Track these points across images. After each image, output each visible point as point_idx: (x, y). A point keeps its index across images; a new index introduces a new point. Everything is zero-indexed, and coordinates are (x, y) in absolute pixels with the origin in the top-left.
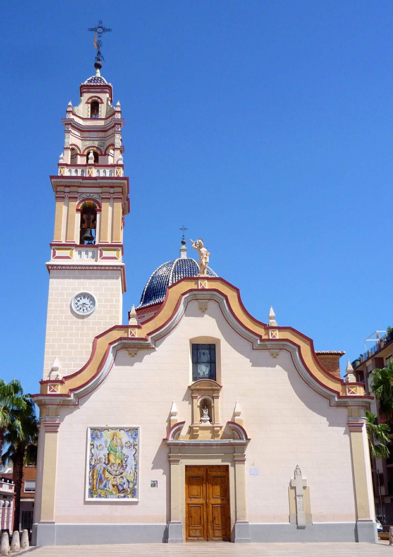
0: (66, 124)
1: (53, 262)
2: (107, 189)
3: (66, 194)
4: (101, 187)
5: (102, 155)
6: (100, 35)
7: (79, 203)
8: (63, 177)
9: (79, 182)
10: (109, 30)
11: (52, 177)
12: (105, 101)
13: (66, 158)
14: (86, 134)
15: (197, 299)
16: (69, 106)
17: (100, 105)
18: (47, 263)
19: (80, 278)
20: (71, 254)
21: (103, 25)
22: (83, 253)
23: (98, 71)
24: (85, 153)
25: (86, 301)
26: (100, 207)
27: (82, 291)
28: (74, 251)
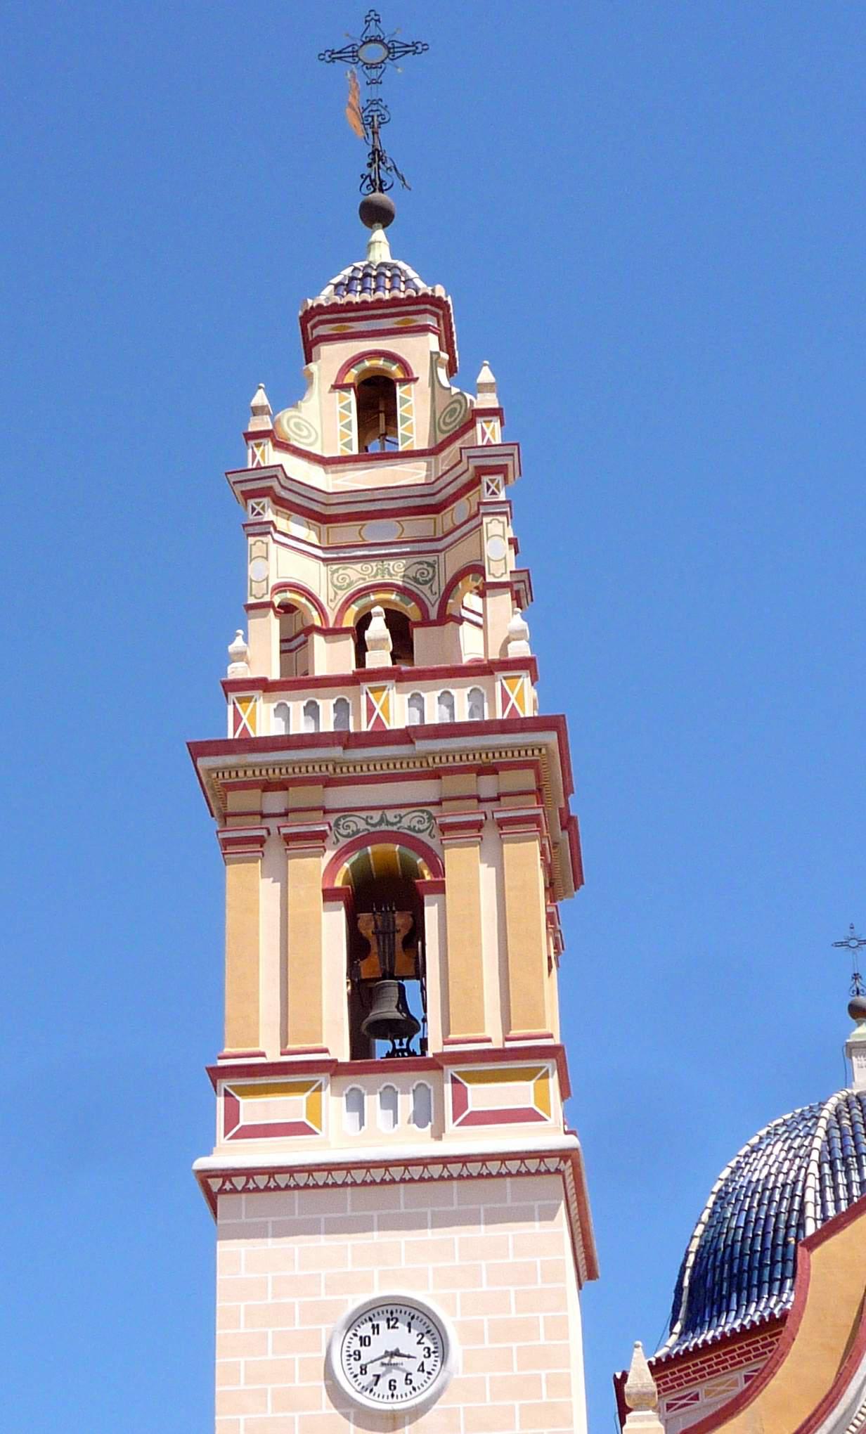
0: (248, 495)
1: (229, 1154)
2: (465, 784)
3: (272, 823)
4: (436, 775)
5: (426, 622)
6: (374, 73)
7: (337, 860)
9: (326, 761)
10: (413, 48)
11: (198, 750)
12: (421, 369)
13: (259, 649)
14: (347, 533)
16: (257, 411)
17: (400, 391)
18: (202, 1163)
19: (362, 1226)
20: (315, 1110)
21: (387, 30)
22: (372, 1102)
23: (379, 235)
24: (349, 622)
25: (402, 1338)
26: (438, 870)
27: (378, 1292)
28: (326, 1093)
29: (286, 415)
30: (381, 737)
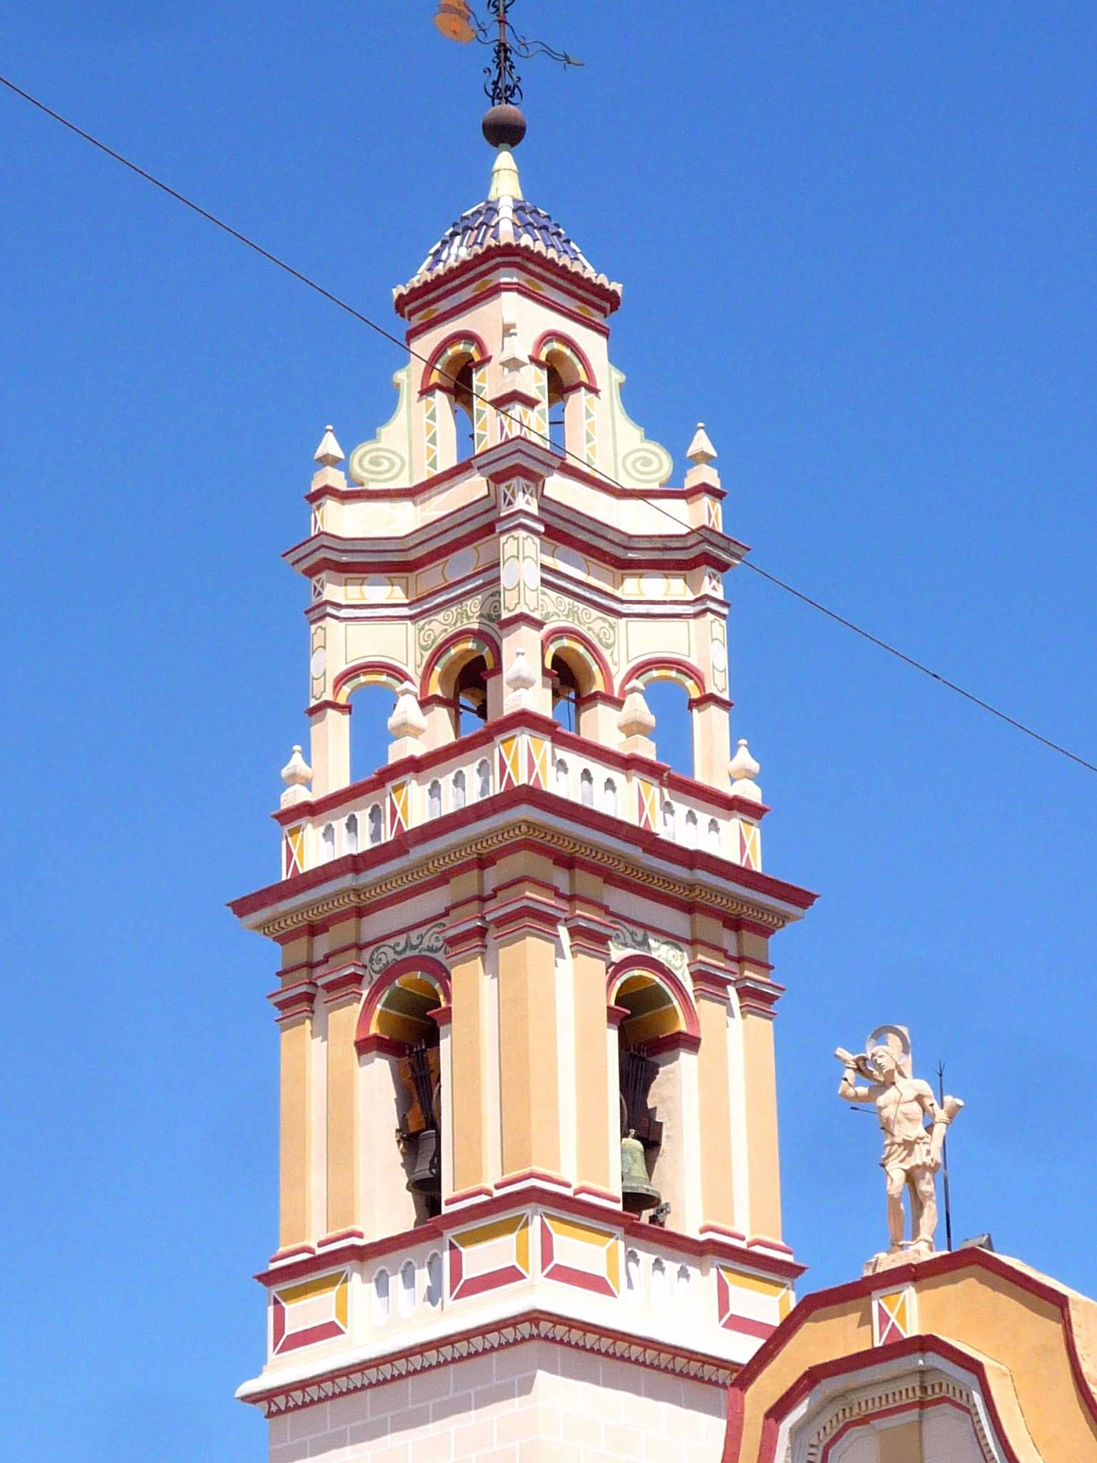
0: (311, 572)
1: (283, 1369)
2: (467, 884)
8: (303, 882)
11: (242, 907)
14: (431, 577)
15: (865, 1420)
16: (327, 460)
22: (396, 1281)
23: (505, 160)
29: (363, 452)
30: (404, 842)
